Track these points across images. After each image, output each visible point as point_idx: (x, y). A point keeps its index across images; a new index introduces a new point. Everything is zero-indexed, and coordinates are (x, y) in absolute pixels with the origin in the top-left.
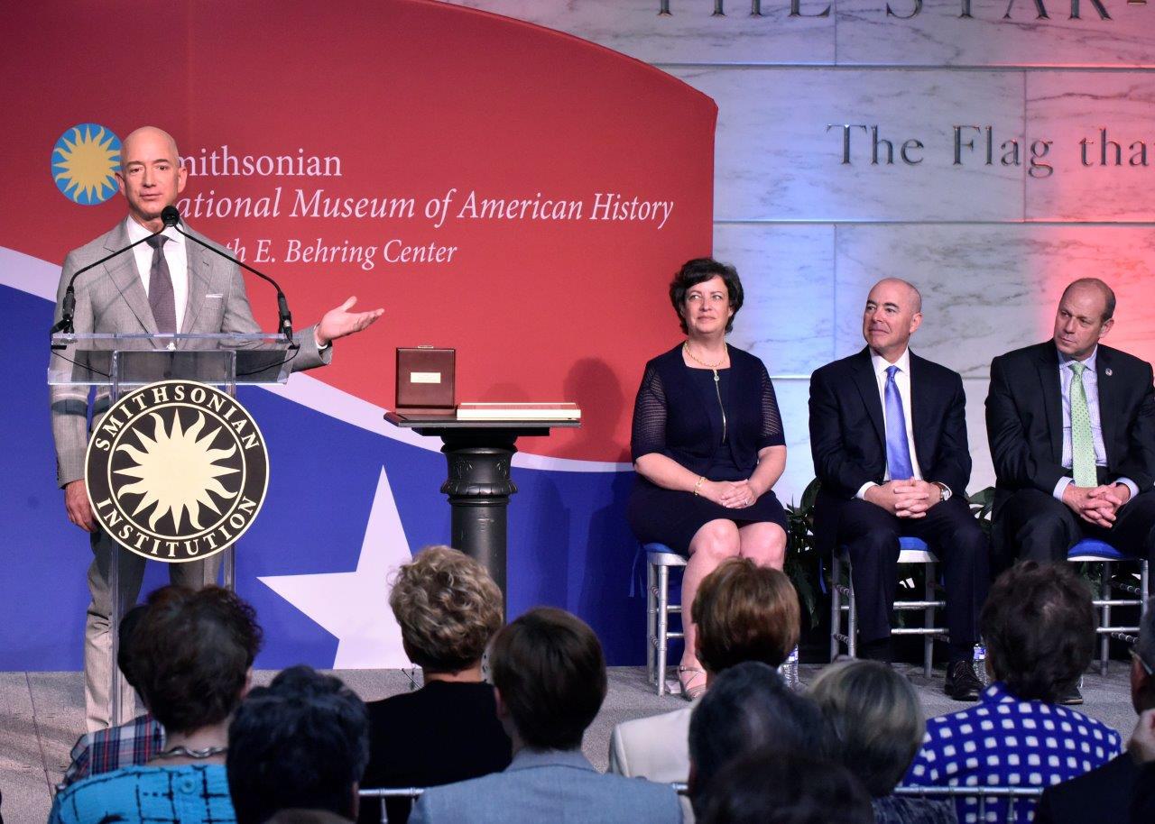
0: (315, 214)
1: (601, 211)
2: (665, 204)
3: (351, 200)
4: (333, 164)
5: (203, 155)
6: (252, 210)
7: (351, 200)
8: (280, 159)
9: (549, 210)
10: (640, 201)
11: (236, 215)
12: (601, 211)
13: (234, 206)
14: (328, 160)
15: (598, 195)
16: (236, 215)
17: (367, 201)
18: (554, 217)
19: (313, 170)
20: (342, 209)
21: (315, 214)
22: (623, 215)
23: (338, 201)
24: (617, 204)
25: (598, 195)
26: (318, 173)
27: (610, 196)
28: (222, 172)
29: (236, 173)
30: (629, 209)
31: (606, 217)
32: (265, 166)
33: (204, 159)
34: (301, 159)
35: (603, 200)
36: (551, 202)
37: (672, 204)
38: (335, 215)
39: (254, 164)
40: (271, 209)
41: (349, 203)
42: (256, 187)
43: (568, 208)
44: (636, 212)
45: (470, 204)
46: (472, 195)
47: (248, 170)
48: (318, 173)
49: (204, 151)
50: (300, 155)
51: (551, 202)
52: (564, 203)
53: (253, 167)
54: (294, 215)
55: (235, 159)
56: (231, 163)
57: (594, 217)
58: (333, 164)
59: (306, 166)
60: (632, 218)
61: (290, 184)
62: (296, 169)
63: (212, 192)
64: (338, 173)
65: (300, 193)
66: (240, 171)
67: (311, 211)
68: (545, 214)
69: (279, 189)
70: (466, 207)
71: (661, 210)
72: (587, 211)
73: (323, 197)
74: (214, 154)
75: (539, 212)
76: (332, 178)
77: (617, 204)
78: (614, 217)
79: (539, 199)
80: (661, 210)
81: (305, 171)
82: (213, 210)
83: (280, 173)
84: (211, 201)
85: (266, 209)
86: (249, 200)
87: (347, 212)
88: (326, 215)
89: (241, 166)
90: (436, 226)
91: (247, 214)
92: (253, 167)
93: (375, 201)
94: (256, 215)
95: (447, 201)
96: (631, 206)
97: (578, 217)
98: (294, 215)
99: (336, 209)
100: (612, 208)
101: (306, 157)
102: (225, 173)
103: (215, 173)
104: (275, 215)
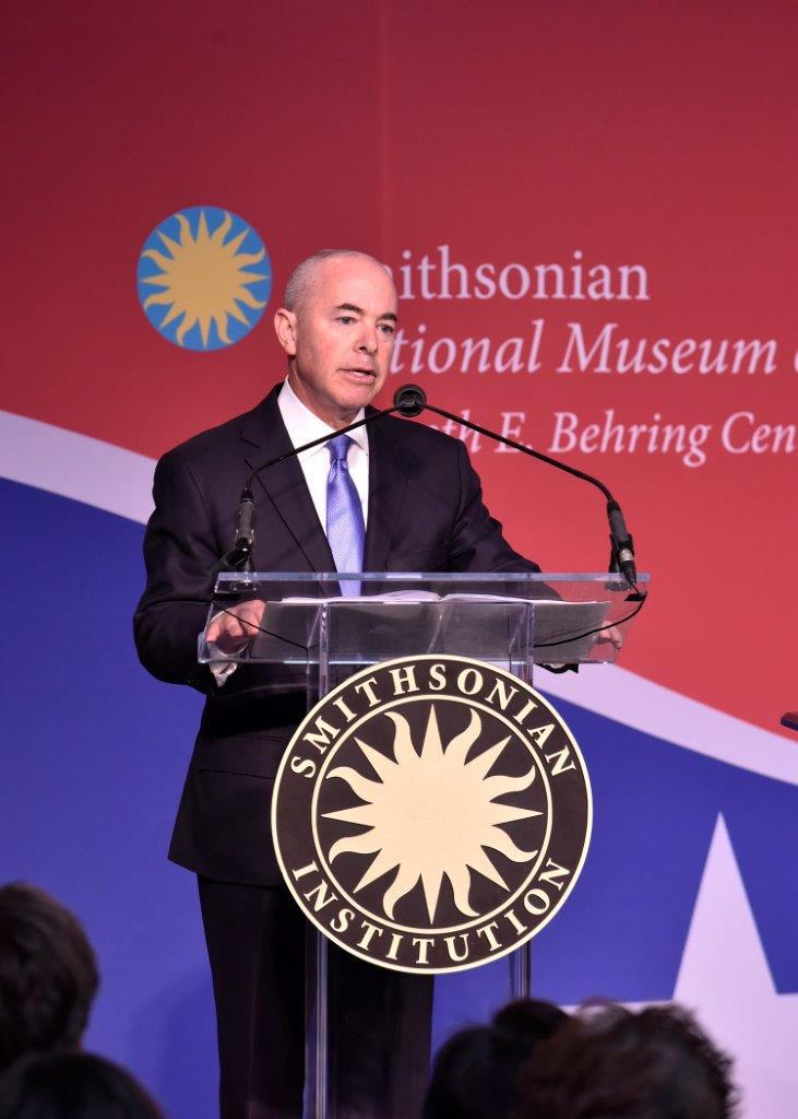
0: (603, 368)
3: (666, 343)
4: (634, 278)
5: (406, 262)
6: (491, 359)
7: (666, 343)
8: (541, 270)
11: (464, 368)
13: (460, 352)
14: (625, 271)
16: (464, 368)
17: (692, 344)
19: (599, 289)
20: (649, 358)
21: (603, 368)
23: (642, 344)
26: (608, 295)
29: (464, 294)
33: (407, 270)
34: (577, 270)
38: (638, 369)
39: (496, 279)
40: (525, 358)
41: (662, 348)
42: (501, 319)
47: (485, 290)
48: (608, 295)
49: (407, 255)
50: (576, 262)
53: (493, 283)
54: (565, 368)
55: (462, 270)
56: (454, 276)
58: (634, 278)
59: (586, 281)
61: (559, 314)
62: (569, 288)
63: (422, 329)
64: (643, 295)
65: (576, 329)
66: (471, 290)
67: (595, 361)
69: (539, 324)
73: (616, 338)
74: (425, 261)
76: (633, 304)
81: (584, 290)
82: (424, 359)
83: (541, 294)
84: (419, 344)
85: (517, 358)
87: (657, 363)
88: (621, 368)
89: (473, 282)
91: (483, 367)
92: (493, 283)
93: (707, 345)
94: (499, 368)
98: (565, 368)
99: (638, 357)
102: (445, 294)
104: (532, 367)
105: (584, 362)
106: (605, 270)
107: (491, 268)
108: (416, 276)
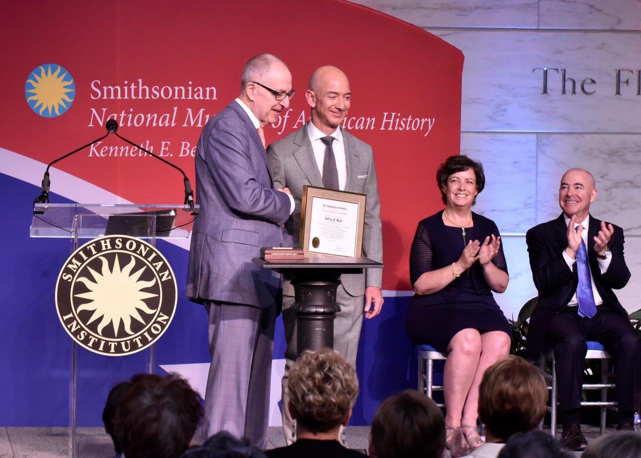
1: (387, 124)
2: (429, 120)
4: (211, 92)
5: (125, 85)
6: (157, 122)
8: (176, 88)
9: (353, 123)
10: (413, 118)
11: (147, 125)
12: (387, 124)
13: (146, 119)
14: (208, 89)
15: (386, 114)
16: (147, 125)
19: (198, 96)
22: (402, 127)
24: (398, 120)
25: (386, 114)
26: (201, 98)
28: (138, 96)
29: (147, 97)
30: (406, 123)
31: (390, 129)
32: (166, 92)
33: (126, 88)
34: (190, 88)
35: (389, 117)
36: (354, 118)
37: (434, 119)
39: (159, 92)
40: (170, 121)
42: (161, 107)
43: (366, 122)
44: (410, 125)
45: (301, 119)
46: (303, 113)
47: (155, 95)
48: (201, 98)
49: (126, 82)
50: (190, 86)
51: (354, 118)
52: (363, 119)
53: (159, 93)
54: (185, 125)
55: (146, 88)
56: (144, 90)
57: (382, 128)
58: (211, 92)
60: (408, 129)
61: (183, 105)
62: (187, 95)
63: (131, 110)
64: (215, 98)
65: (190, 110)
66: (150, 96)
68: (351, 126)
69: (176, 108)
70: (298, 121)
71: (426, 124)
72: (378, 124)
73: (204, 114)
74: (133, 84)
75: (346, 124)
76: (211, 101)
77: (398, 120)
78: (396, 129)
81: (193, 96)
83: (176, 97)
84: (130, 116)
85: (167, 121)
86: (156, 115)
89: (151, 92)
90: (279, 133)
92: (159, 93)
94: (161, 125)
95: (286, 117)
96: (407, 121)
97: (372, 128)
98: (185, 125)
100: (394, 123)
101: (193, 86)
102: (140, 97)
103: (133, 97)
104: (173, 125)
105: (192, 123)
106: (201, 89)
107: (158, 87)
108: (129, 90)
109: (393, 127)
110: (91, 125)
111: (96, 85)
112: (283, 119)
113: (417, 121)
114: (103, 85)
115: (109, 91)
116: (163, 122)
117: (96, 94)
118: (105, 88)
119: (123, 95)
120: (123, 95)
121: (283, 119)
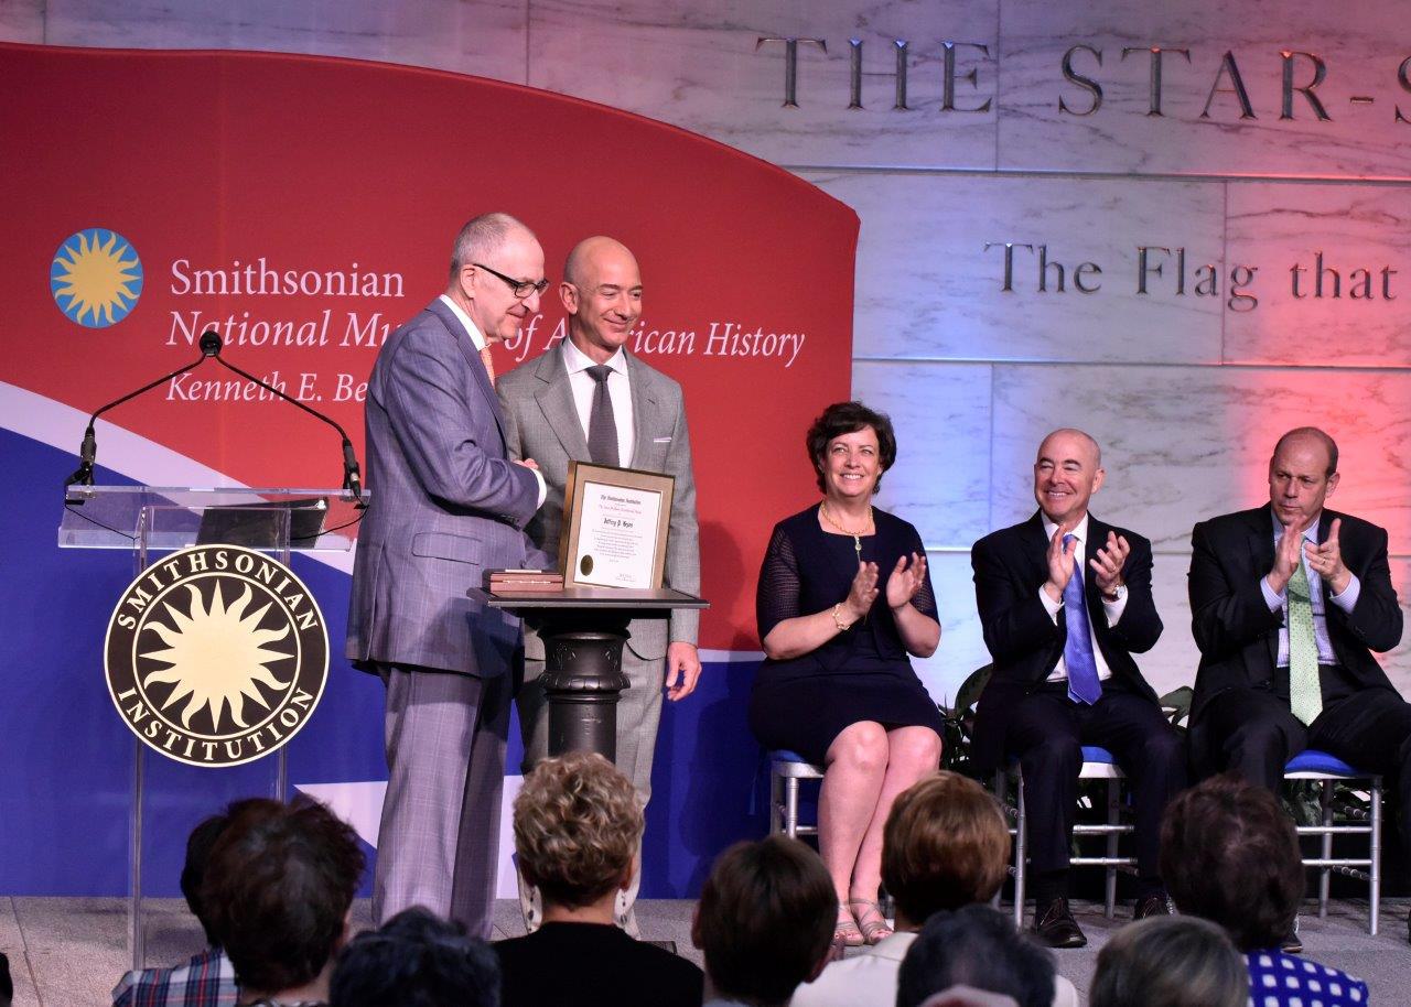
1: (718, 345)
2: (795, 337)
4: (394, 282)
5: (235, 269)
6: (294, 336)
8: (329, 276)
10: (765, 333)
11: (275, 342)
12: (718, 345)
13: (273, 332)
14: (387, 277)
15: (714, 325)
16: (275, 342)
18: (661, 351)
19: (370, 289)
24: (737, 336)
25: (714, 325)
26: (375, 293)
27: (729, 326)
28: (259, 289)
29: (276, 291)
30: (751, 342)
31: (723, 352)
32: (311, 283)
33: (236, 274)
34: (355, 276)
35: (720, 332)
36: (657, 333)
37: (803, 336)
39: (298, 283)
40: (317, 336)
42: (300, 309)
43: (677, 340)
44: (760, 347)
47: (290, 288)
48: (375, 293)
50: (354, 271)
51: (657, 333)
52: (673, 334)
53: (296, 284)
54: (345, 344)
56: (269, 279)
57: (708, 352)
58: (394, 282)
60: (755, 353)
61: (342, 306)
62: (348, 288)
63: (246, 315)
64: (400, 294)
65: (353, 317)
66: (280, 289)
67: (366, 339)
68: (650, 348)
69: (328, 312)
70: (554, 337)
71: (789, 344)
72: (701, 343)
73: (380, 323)
74: (249, 268)
75: (642, 344)
76: (393, 299)
77: (737, 336)
78: (733, 352)
79: (644, 329)
80: (789, 344)
81: (359, 290)
82: (247, 336)
84: (244, 325)
85: (312, 336)
86: (290, 325)
89: (282, 283)
91: (288, 342)
92: (296, 284)
94: (300, 342)
95: (531, 329)
97: (690, 351)
98: (345, 344)
101: (361, 272)
102: (263, 291)
103: (250, 291)
104: (322, 343)
105: (358, 340)
107: (295, 273)
108: (243, 278)
109: (729, 349)
110: (171, 342)
111: (181, 268)
112: (525, 334)
113: (771, 339)
114: (194, 267)
115: (205, 279)
116: (303, 338)
117: (181, 285)
118: (198, 275)
119: (230, 286)
120: (230, 286)
121: (525, 334)
